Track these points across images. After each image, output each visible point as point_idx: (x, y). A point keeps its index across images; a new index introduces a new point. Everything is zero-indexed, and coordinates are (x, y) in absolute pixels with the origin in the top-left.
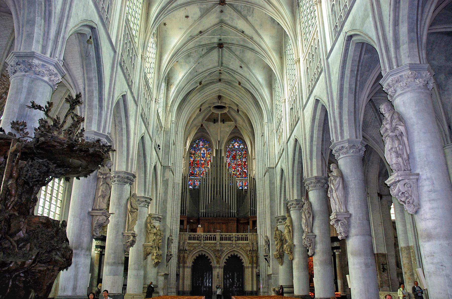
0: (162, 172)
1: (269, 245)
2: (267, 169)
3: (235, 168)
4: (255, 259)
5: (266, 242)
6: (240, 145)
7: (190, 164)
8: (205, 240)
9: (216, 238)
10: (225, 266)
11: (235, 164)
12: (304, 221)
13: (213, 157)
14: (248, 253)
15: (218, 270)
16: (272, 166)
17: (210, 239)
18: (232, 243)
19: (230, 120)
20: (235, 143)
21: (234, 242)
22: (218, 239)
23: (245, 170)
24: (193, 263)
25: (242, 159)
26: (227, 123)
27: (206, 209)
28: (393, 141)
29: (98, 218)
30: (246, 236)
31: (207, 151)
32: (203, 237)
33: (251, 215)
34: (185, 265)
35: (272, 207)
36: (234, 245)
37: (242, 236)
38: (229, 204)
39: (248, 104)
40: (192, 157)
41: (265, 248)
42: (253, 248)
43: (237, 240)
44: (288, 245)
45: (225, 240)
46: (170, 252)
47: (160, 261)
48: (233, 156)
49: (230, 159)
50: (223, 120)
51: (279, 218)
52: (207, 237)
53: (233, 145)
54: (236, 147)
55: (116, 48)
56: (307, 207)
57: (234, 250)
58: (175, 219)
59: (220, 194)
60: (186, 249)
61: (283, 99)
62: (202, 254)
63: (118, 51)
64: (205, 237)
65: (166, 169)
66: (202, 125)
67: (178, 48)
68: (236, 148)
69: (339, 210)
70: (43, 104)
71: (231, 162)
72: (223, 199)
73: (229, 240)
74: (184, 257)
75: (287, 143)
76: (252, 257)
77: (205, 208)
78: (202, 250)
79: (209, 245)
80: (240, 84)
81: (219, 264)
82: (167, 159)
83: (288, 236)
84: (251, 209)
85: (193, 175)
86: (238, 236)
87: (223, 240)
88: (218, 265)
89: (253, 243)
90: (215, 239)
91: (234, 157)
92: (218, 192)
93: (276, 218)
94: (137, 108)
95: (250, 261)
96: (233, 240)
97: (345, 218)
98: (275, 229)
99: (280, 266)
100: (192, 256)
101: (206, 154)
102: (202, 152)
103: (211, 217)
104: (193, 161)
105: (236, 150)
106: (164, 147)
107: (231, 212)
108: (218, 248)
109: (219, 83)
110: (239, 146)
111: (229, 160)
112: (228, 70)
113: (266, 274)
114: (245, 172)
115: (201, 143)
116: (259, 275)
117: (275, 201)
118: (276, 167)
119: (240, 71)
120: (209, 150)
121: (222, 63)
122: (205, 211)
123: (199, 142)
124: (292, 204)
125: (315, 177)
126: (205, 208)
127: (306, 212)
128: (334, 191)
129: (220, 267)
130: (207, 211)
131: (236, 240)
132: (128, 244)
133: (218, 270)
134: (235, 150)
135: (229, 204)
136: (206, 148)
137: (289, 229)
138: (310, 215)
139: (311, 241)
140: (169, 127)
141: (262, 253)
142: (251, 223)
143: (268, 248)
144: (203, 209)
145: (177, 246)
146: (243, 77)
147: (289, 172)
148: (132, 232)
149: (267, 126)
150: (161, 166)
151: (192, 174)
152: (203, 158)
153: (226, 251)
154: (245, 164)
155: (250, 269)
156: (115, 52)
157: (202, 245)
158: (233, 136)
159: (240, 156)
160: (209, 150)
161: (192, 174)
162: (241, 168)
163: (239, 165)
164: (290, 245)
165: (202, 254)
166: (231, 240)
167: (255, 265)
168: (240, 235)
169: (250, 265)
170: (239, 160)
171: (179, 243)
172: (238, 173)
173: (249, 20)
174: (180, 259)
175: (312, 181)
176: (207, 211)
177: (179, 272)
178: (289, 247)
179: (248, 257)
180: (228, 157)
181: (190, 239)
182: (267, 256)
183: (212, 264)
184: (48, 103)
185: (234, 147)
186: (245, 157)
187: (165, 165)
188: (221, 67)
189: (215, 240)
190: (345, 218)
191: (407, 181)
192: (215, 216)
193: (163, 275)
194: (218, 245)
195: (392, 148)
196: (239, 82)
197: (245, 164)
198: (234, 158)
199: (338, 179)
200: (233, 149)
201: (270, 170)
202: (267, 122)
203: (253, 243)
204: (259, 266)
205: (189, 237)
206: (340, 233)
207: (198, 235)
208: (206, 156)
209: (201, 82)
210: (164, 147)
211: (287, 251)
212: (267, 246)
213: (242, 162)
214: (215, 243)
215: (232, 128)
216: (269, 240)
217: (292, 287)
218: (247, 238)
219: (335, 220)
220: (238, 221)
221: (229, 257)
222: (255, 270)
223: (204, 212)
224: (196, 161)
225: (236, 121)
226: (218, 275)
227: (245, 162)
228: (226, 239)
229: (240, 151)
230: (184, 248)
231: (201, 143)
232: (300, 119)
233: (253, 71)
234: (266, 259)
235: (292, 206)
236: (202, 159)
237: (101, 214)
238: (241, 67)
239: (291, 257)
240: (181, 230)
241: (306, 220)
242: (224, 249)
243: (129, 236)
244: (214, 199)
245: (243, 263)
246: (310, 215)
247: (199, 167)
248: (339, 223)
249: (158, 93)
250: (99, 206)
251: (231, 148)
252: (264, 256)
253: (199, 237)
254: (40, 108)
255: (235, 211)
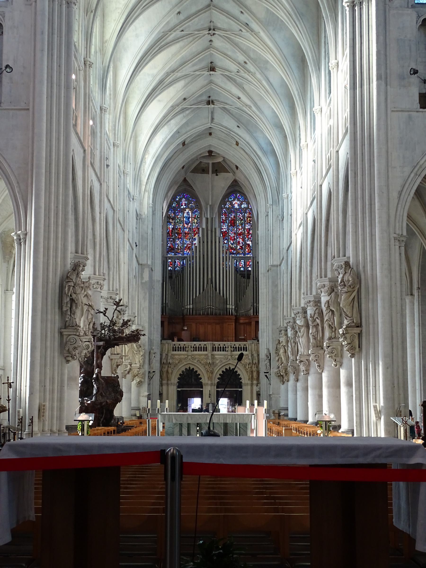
0: (140, 272)
1: (270, 360)
2: (270, 267)
3: (235, 239)
4: (255, 374)
5: (267, 356)
6: (241, 204)
7: (168, 233)
8: (194, 351)
9: (206, 347)
10: (218, 382)
11: (235, 233)
12: (290, 350)
13: (203, 229)
14: (247, 367)
15: (209, 388)
16: (275, 263)
17: (200, 349)
18: (227, 355)
19: (227, 171)
20: (234, 200)
21: (229, 352)
22: (210, 349)
23: (248, 243)
24: (179, 379)
25: (245, 226)
26: (222, 175)
27: (193, 304)
28: (313, 329)
29: (116, 361)
30: (245, 345)
31: (192, 213)
32: (191, 347)
33: (254, 314)
34: (169, 382)
35: (274, 315)
36: (229, 357)
37: (240, 345)
38: (225, 297)
39: (249, 169)
40: (170, 223)
41: (266, 362)
42: (253, 361)
43: (234, 351)
44: (283, 366)
45: (218, 351)
46: (152, 369)
47: (143, 380)
48: (231, 220)
49: (227, 225)
50: (216, 170)
51: (282, 329)
52: (196, 347)
53: (231, 204)
54: (236, 206)
55: (114, 206)
56: (293, 337)
57: (230, 364)
58: (155, 327)
59: (212, 283)
60: (169, 363)
61: (285, 194)
62: (190, 368)
63: (115, 209)
64: (194, 347)
65: (144, 269)
66: (185, 180)
67: (157, 125)
68: (236, 209)
69: (303, 354)
70: (102, 310)
71: (228, 229)
72: (216, 290)
73: (223, 351)
74: (167, 372)
75: (287, 250)
76: (252, 372)
77: (191, 303)
78: (189, 363)
79: (198, 356)
80: (237, 144)
81: (211, 381)
82: (146, 256)
83: (284, 356)
84: (254, 306)
85: (173, 250)
86: (235, 345)
87: (216, 351)
88: (209, 382)
89: (252, 355)
90: (205, 349)
91: (232, 222)
92: (210, 281)
93: (278, 328)
94: (124, 234)
95: (249, 377)
96: (228, 351)
97: (307, 360)
98: (277, 342)
99: (281, 385)
100: (178, 371)
101: (192, 218)
102: (185, 215)
103: (200, 315)
104: (173, 229)
105: (236, 211)
106: (140, 240)
107: (227, 308)
108: (210, 361)
109: (210, 138)
110: (240, 205)
111: (225, 228)
112: (222, 127)
113: (267, 394)
114: (249, 245)
115: (184, 201)
116: (260, 395)
117: (278, 308)
118: (280, 265)
119: (236, 130)
120: (196, 211)
121: (213, 119)
122: (191, 307)
123: (180, 200)
124: (290, 322)
125: (302, 307)
126: (191, 303)
127: (292, 341)
128: (300, 338)
129: (212, 385)
130: (194, 307)
131: (232, 351)
132: (126, 372)
133: (209, 388)
134: (234, 212)
135: (225, 297)
136: (191, 209)
137: (285, 349)
138: (295, 344)
139: (295, 368)
140: (146, 213)
141: (263, 368)
142: (253, 323)
143: (268, 364)
144: (188, 304)
145: (159, 359)
146: (241, 139)
147: (287, 285)
148: (129, 361)
149: (271, 209)
150: (139, 264)
151: (171, 249)
152: (186, 224)
153: (219, 364)
154: (248, 233)
155: (249, 387)
156: (114, 211)
157: (190, 357)
158: (232, 189)
159: (242, 220)
160: (196, 211)
161: (171, 249)
162: (243, 240)
163: (240, 234)
164: (285, 366)
165: (190, 368)
166: (225, 351)
167: (255, 382)
168: (237, 344)
169: (249, 382)
170: (240, 227)
171: (161, 355)
172: (239, 247)
173: (246, 89)
174: (163, 374)
175: (299, 311)
176: (194, 307)
177: (162, 391)
178: (284, 368)
179: (247, 372)
180: (224, 223)
181: (174, 349)
182: (268, 373)
183: (202, 380)
184: (105, 308)
185: (233, 206)
186: (250, 223)
187: (143, 263)
188: (212, 124)
189: (206, 351)
190: (307, 360)
191: (317, 354)
192: (206, 313)
193: (146, 396)
194: (210, 358)
195: (311, 333)
196: (237, 142)
197: (248, 233)
198: (233, 223)
199: (303, 329)
200: (232, 210)
201: (273, 268)
202: (271, 203)
203: (252, 355)
204: (260, 383)
205: (173, 347)
206: (303, 371)
207: (185, 345)
208: (192, 221)
209: (184, 142)
210: (140, 240)
211: (282, 372)
212: (268, 361)
213: (244, 229)
214: (206, 355)
215: (229, 183)
216: (270, 354)
217: (287, 409)
218: (246, 347)
219: (299, 361)
220: (237, 319)
221: (223, 372)
222: (255, 389)
223: (190, 308)
224: (177, 229)
225: (234, 173)
226: (210, 394)
227: (249, 229)
228: (219, 349)
229: (241, 213)
230: (167, 360)
231: (184, 201)
232: (284, 259)
233: (255, 135)
234: (266, 376)
235: (288, 324)
236: (186, 226)
237: (119, 358)
238: (238, 126)
239: (286, 378)
240: (163, 338)
241: (292, 349)
242: (217, 362)
243: (126, 366)
244: (203, 290)
245: (241, 379)
246: (296, 344)
247: (181, 238)
248: (302, 363)
249: (136, 188)
250: (116, 352)
251: (229, 207)
252: (265, 373)
253: (186, 347)
254: (101, 312)
255: (233, 307)
